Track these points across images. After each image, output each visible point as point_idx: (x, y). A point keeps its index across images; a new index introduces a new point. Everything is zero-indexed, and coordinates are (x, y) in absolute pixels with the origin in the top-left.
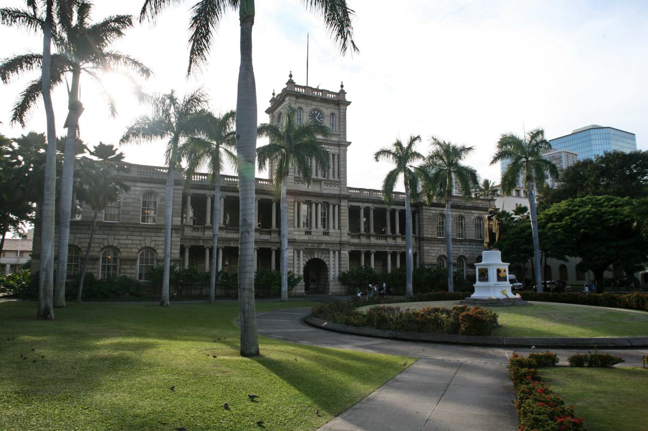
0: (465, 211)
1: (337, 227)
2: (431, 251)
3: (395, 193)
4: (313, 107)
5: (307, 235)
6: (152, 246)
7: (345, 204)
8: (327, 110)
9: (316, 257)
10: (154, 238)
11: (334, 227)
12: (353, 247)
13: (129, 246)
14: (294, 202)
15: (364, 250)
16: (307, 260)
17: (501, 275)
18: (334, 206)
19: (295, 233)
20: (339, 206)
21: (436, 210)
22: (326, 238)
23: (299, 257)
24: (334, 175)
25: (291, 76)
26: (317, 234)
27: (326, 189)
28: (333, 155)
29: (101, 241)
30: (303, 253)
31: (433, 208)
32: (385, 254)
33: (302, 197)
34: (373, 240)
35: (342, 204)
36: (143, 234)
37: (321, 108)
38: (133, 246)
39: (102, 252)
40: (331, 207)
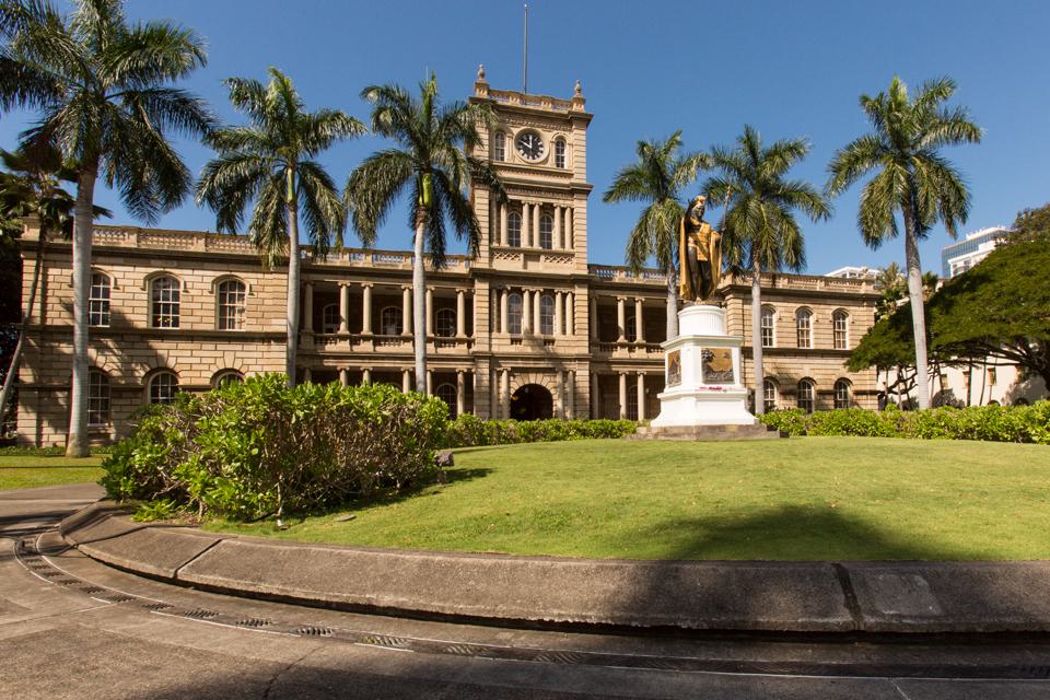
4: (523, 128)
6: (237, 367)
7: (582, 293)
9: (532, 382)
10: (238, 354)
13: (194, 367)
18: (564, 296)
20: (573, 295)
27: (546, 267)
28: (563, 210)
34: (640, 354)
37: (540, 130)
38: (202, 367)
39: (151, 379)
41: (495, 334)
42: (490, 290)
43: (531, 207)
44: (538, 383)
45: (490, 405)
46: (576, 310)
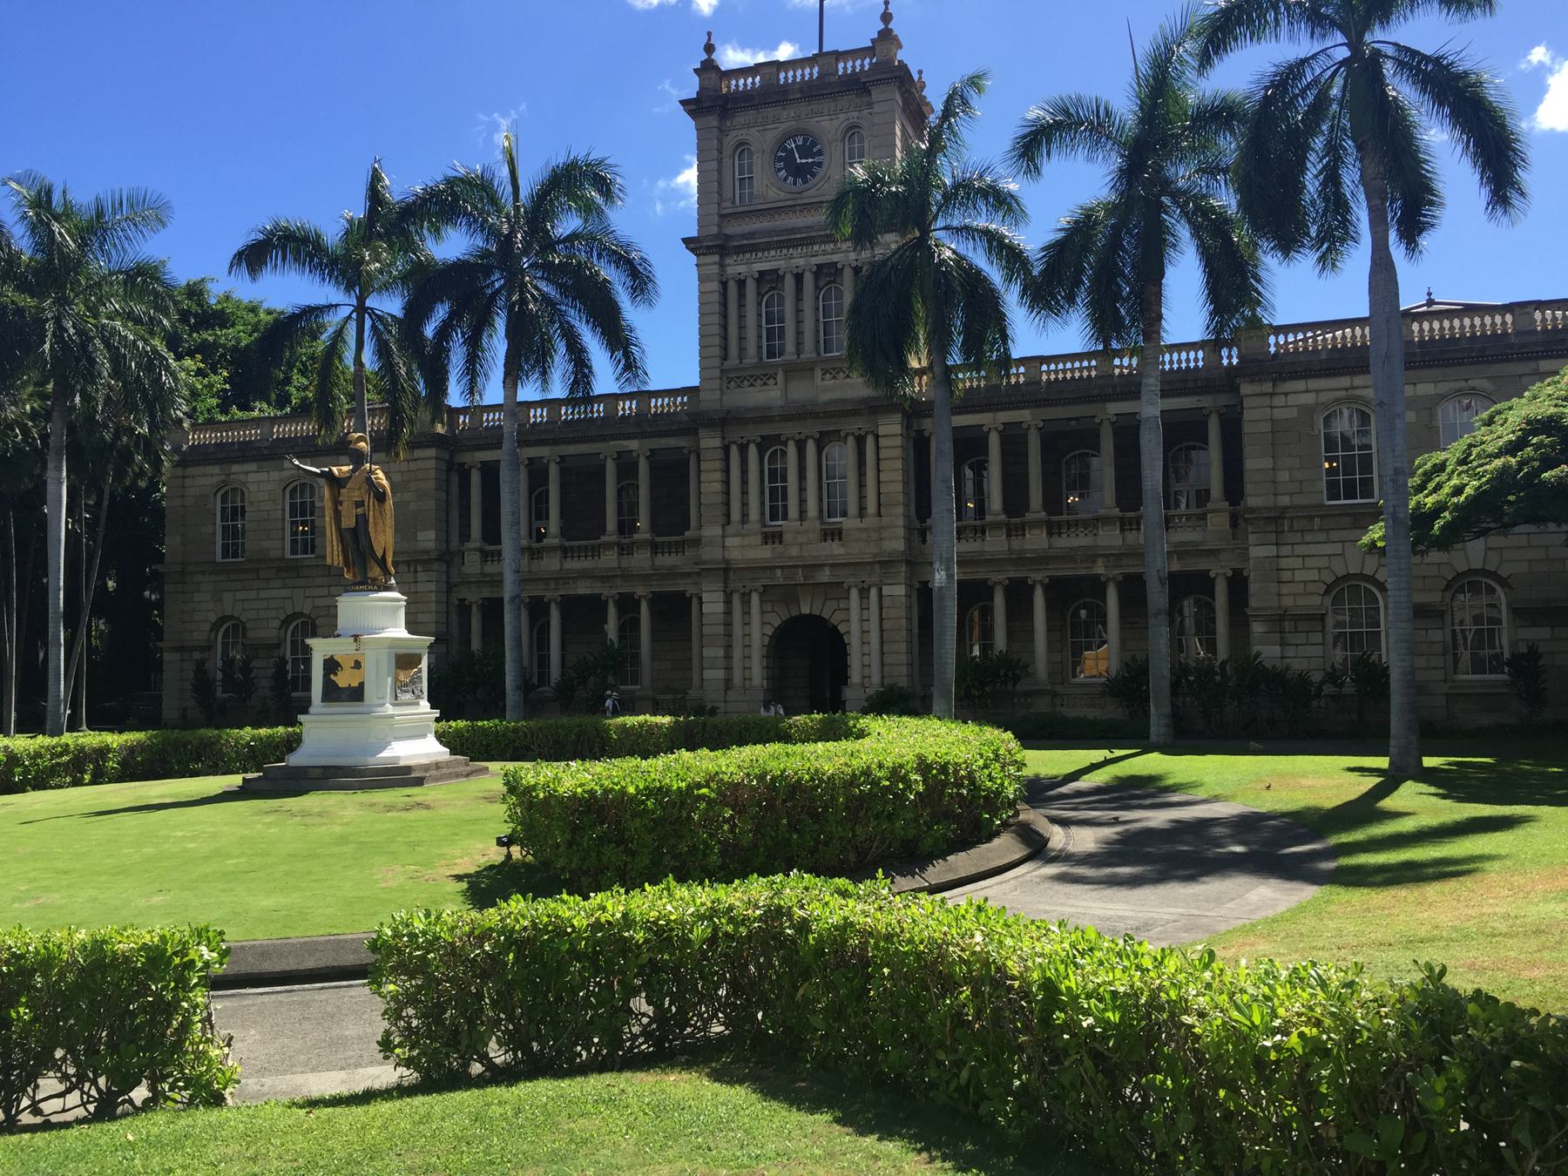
0: (1497, 369)
1: (871, 507)
2: (1284, 563)
3: (1023, 361)
4: (783, 127)
5: (769, 547)
8: (828, 123)
9: (805, 610)
15: (1002, 577)
17: (343, 680)
18: (860, 442)
19: (729, 542)
20: (877, 437)
21: (1317, 391)
23: (746, 613)
30: (762, 602)
31: (1300, 385)
32: (1097, 586)
34: (1036, 540)
35: (882, 431)
40: (851, 440)
41: (731, 529)
43: (799, 278)
44: (816, 612)
45: (728, 657)
46: (883, 465)
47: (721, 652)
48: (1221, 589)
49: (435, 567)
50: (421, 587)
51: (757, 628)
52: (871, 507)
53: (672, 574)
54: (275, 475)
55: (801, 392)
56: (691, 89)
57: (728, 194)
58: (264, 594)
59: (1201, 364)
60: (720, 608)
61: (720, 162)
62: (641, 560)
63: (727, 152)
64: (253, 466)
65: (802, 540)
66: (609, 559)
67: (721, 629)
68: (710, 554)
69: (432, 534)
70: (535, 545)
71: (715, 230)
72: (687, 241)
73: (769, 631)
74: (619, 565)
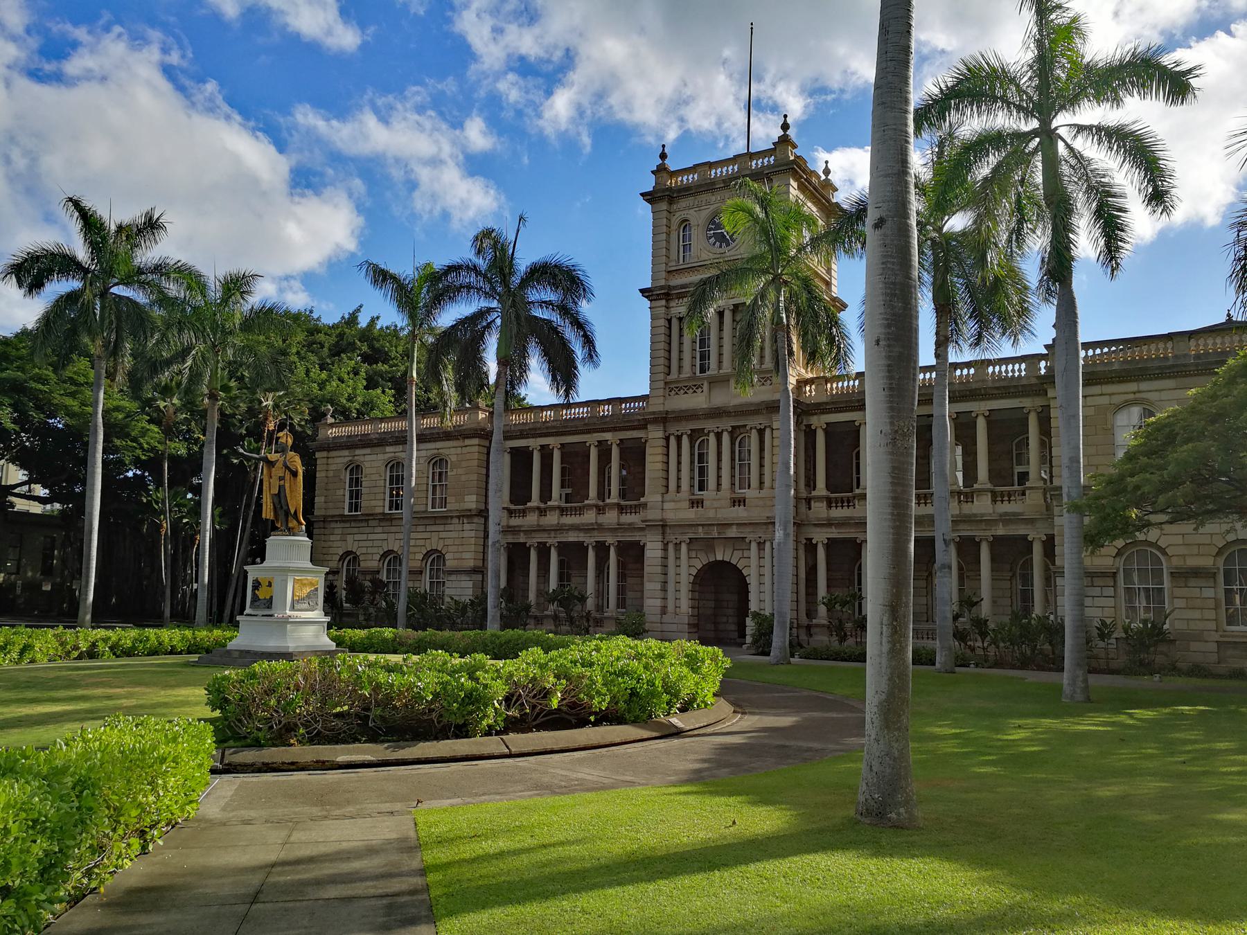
4: (712, 207)
9: (719, 558)
10: (443, 535)
11: (761, 483)
12: (834, 530)
14: (667, 439)
16: (699, 566)
18: (761, 433)
19: (666, 506)
22: (740, 513)
23: (678, 558)
24: (762, 357)
25: (663, 156)
26: (716, 504)
29: (379, 543)
30: (689, 550)
33: (684, 423)
36: (429, 529)
41: (667, 497)
42: (667, 439)
45: (664, 590)
47: (658, 586)
48: (1037, 550)
49: (476, 520)
50: (466, 534)
51: (686, 568)
52: (767, 483)
53: (631, 528)
54: (381, 457)
55: (721, 398)
56: (649, 184)
57: (673, 256)
58: (371, 537)
59: (1023, 373)
60: (659, 553)
61: (668, 234)
62: (611, 517)
63: (674, 227)
64: (368, 451)
65: (716, 505)
66: (589, 517)
67: (659, 570)
68: (653, 514)
69: (474, 498)
70: (542, 505)
71: (663, 283)
72: (642, 291)
73: (694, 572)
74: (596, 521)
